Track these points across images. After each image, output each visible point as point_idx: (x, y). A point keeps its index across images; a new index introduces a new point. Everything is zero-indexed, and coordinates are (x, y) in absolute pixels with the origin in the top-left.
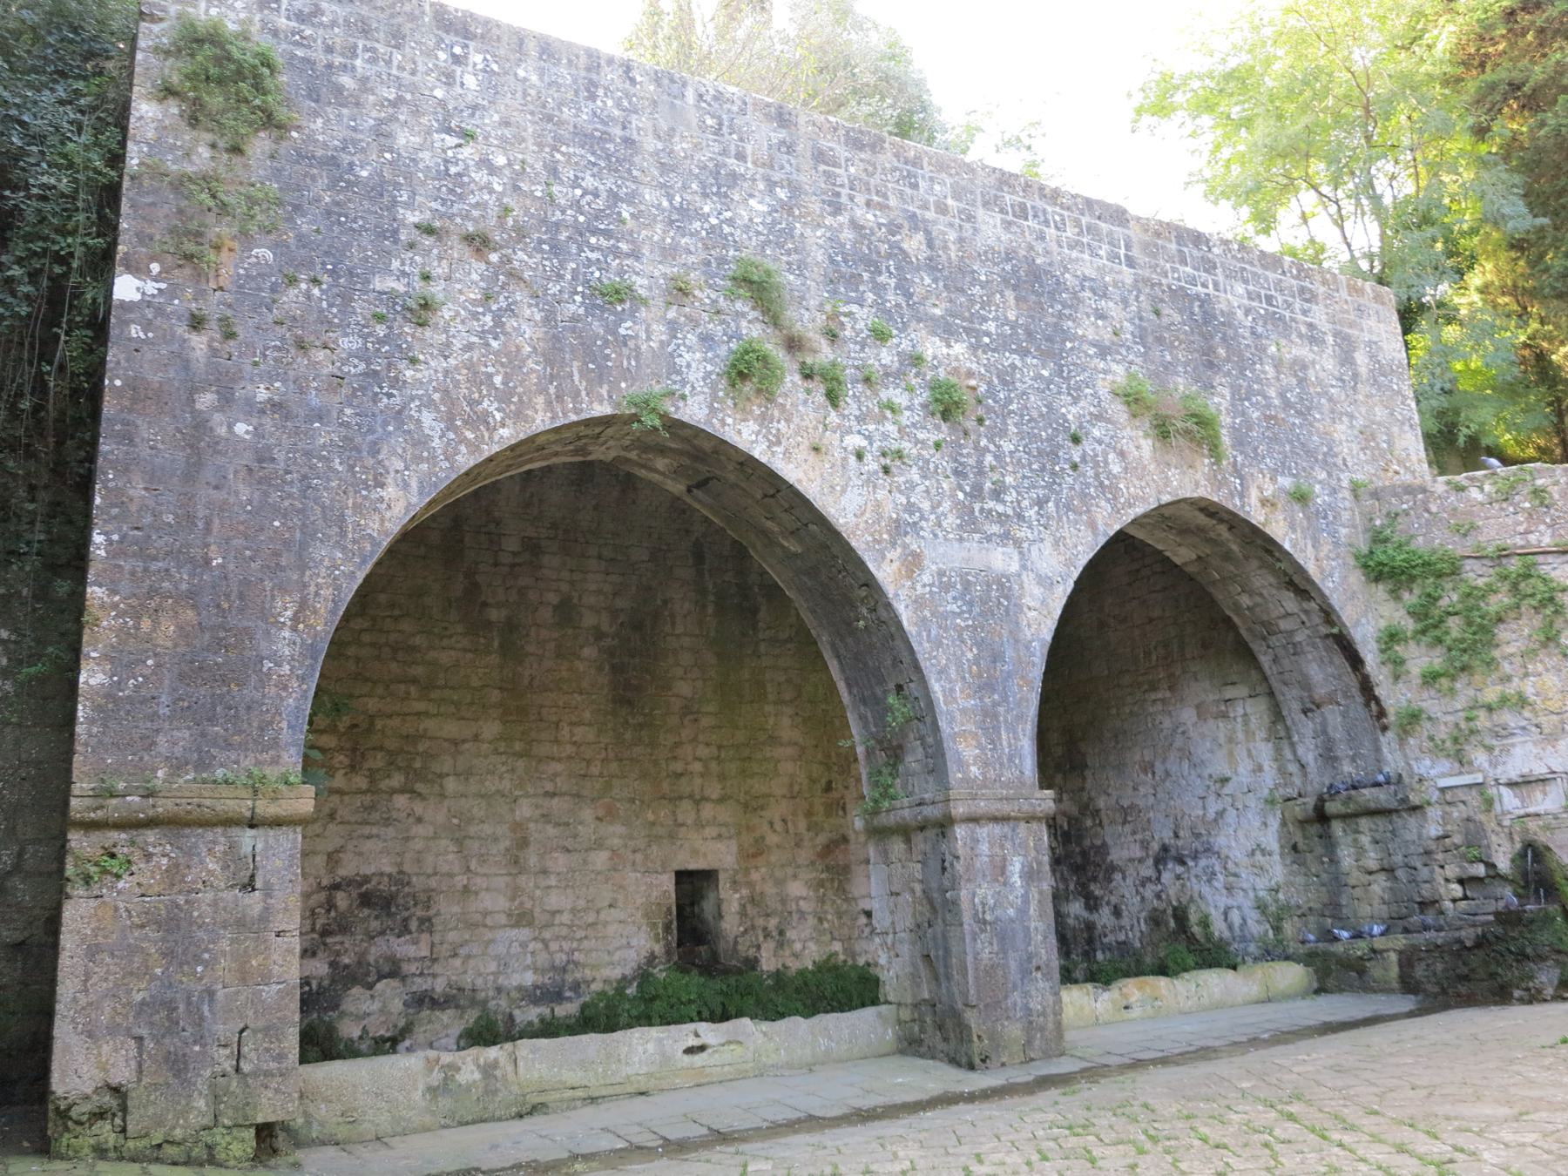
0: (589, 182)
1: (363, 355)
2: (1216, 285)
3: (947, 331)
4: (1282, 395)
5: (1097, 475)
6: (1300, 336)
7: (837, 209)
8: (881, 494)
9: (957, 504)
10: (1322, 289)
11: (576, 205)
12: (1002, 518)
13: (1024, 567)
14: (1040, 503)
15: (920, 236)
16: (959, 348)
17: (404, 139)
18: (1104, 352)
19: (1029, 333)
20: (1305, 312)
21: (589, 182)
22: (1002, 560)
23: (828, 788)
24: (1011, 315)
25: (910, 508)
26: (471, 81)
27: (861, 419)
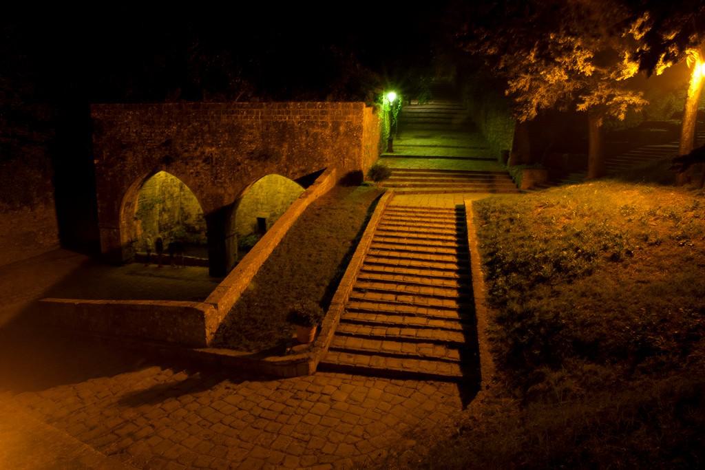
0: (147, 131)
1: (120, 167)
2: (289, 118)
3: (211, 145)
4: (307, 145)
5: (245, 172)
6: (318, 125)
7: (189, 124)
8: (197, 180)
9: (211, 181)
10: (330, 109)
11: (146, 136)
12: (221, 183)
13: (225, 192)
14: (230, 179)
15: (207, 126)
16: (213, 149)
17: (122, 131)
18: (250, 142)
19: (230, 142)
20: (321, 118)
21: (147, 131)
22: (221, 191)
23: (291, 203)
24: (227, 139)
25: (202, 182)
26: (130, 117)
27: (193, 167)
